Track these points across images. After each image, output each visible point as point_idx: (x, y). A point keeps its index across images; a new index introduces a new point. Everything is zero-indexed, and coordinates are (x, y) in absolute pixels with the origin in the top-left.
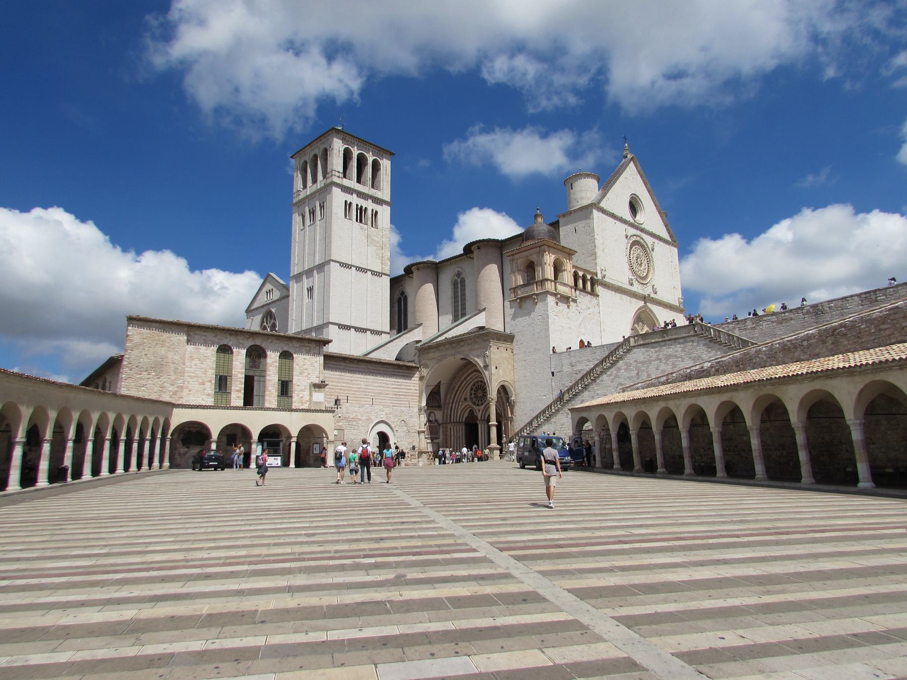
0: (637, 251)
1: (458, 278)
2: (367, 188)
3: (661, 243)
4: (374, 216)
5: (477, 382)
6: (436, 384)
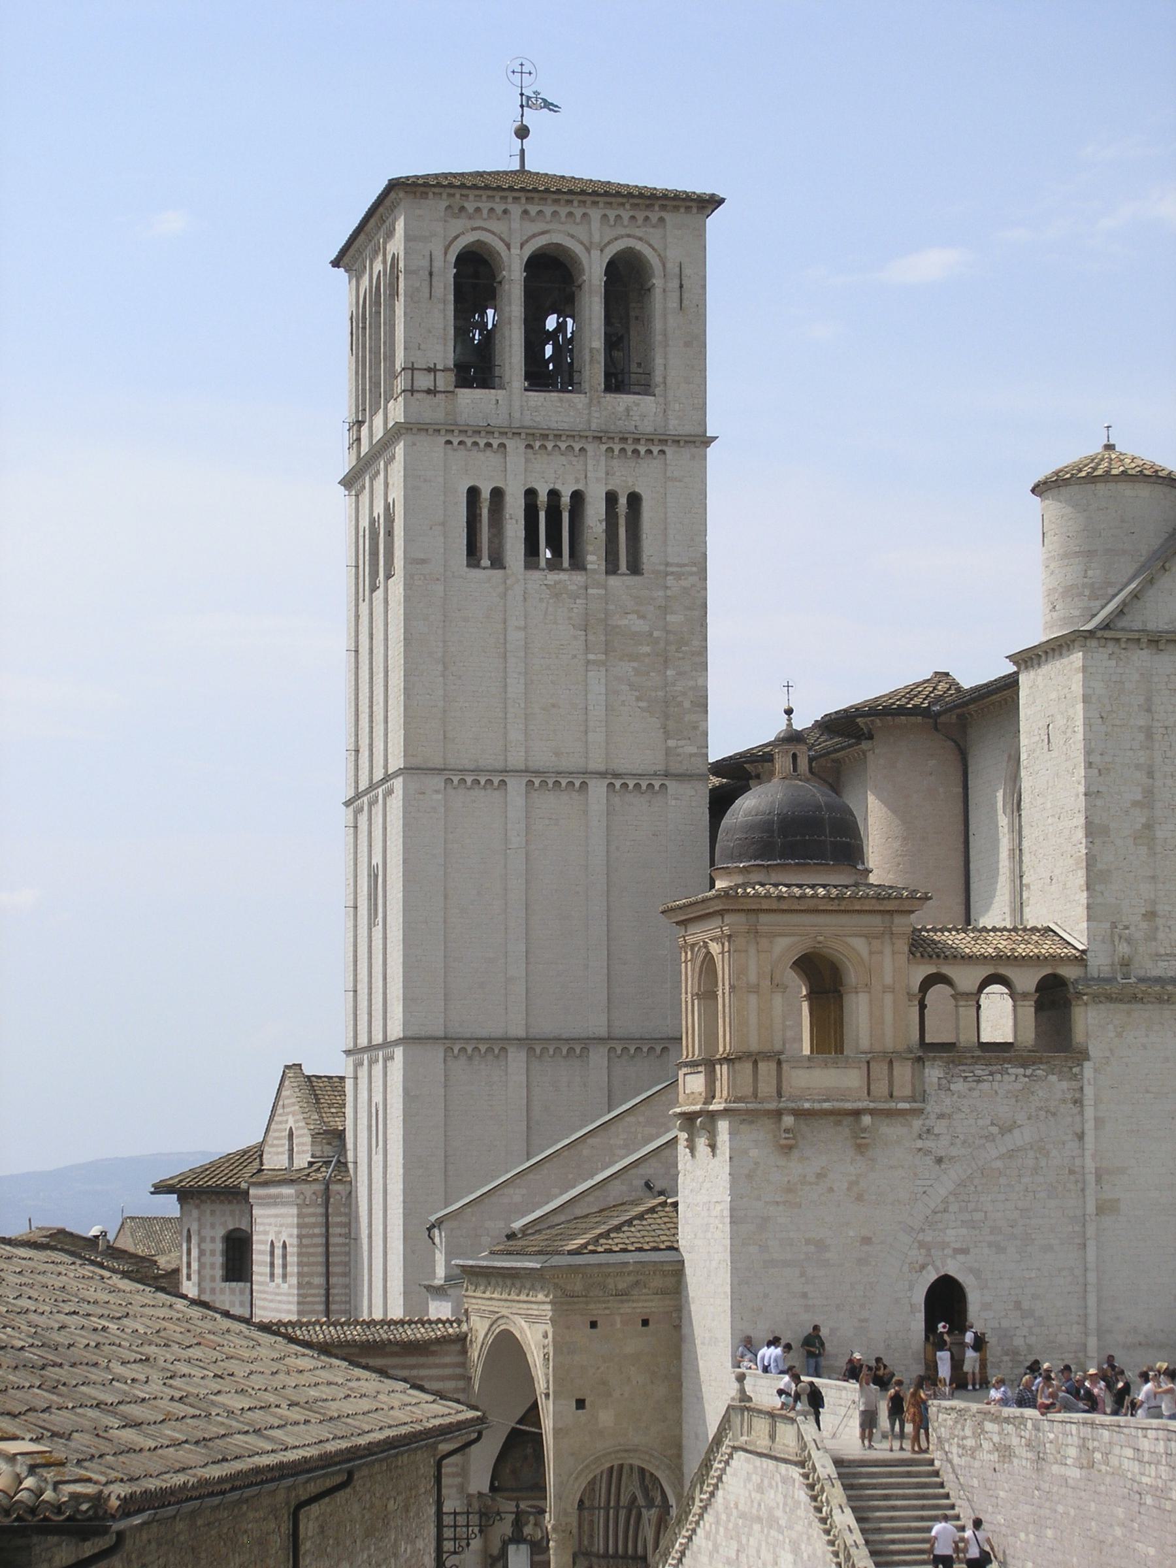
2: (578, 400)
4: (622, 522)
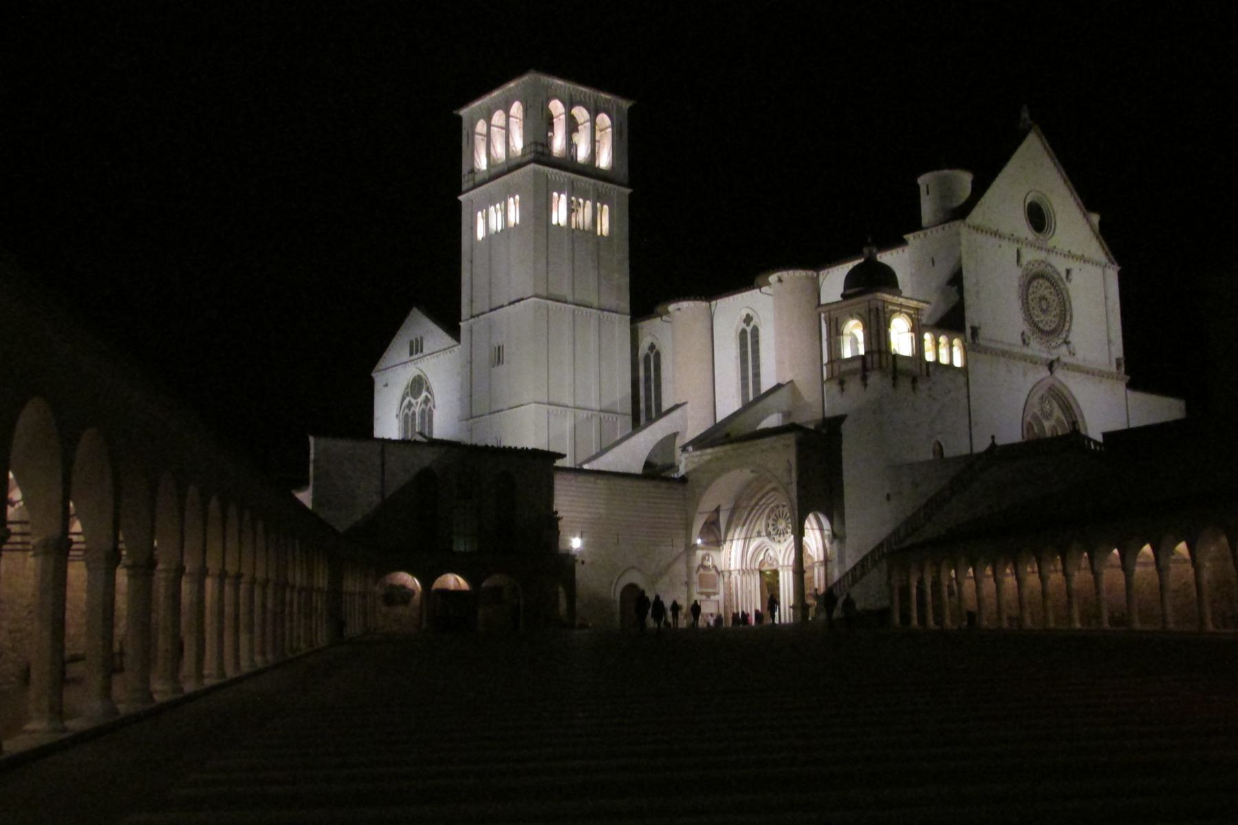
0: (1042, 288)
1: (748, 325)
3: (1088, 267)
5: (778, 507)
6: (713, 509)
